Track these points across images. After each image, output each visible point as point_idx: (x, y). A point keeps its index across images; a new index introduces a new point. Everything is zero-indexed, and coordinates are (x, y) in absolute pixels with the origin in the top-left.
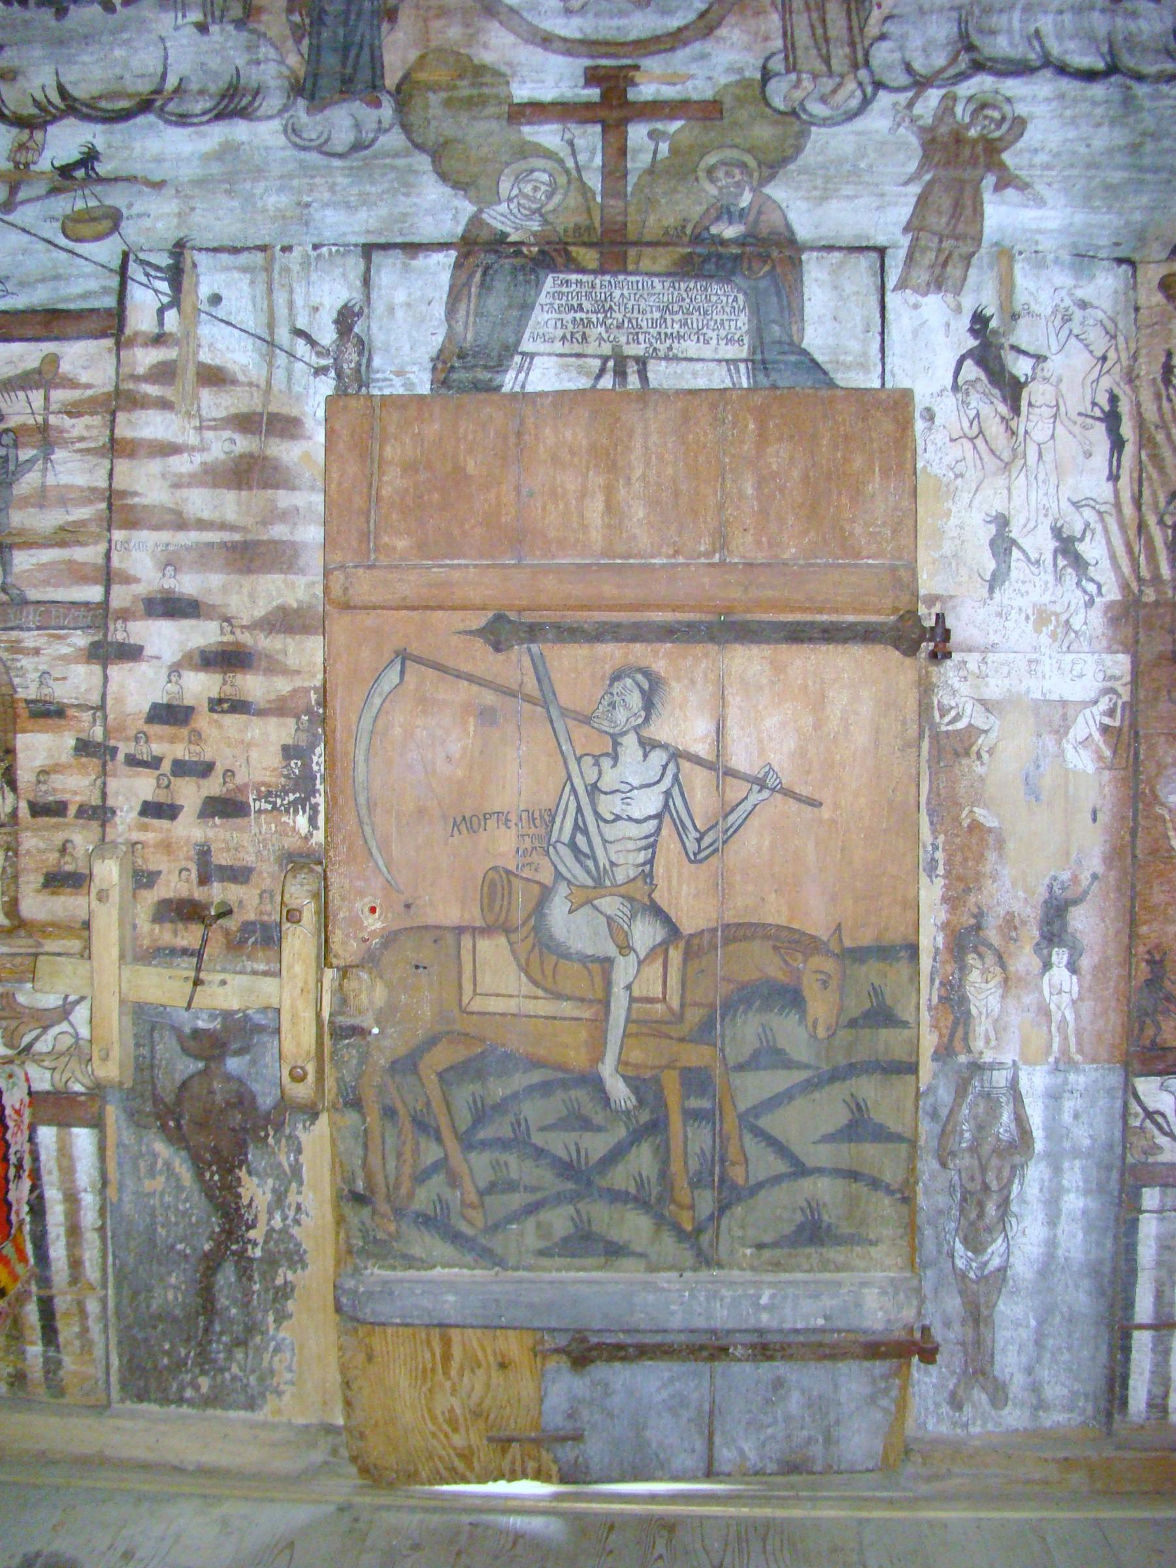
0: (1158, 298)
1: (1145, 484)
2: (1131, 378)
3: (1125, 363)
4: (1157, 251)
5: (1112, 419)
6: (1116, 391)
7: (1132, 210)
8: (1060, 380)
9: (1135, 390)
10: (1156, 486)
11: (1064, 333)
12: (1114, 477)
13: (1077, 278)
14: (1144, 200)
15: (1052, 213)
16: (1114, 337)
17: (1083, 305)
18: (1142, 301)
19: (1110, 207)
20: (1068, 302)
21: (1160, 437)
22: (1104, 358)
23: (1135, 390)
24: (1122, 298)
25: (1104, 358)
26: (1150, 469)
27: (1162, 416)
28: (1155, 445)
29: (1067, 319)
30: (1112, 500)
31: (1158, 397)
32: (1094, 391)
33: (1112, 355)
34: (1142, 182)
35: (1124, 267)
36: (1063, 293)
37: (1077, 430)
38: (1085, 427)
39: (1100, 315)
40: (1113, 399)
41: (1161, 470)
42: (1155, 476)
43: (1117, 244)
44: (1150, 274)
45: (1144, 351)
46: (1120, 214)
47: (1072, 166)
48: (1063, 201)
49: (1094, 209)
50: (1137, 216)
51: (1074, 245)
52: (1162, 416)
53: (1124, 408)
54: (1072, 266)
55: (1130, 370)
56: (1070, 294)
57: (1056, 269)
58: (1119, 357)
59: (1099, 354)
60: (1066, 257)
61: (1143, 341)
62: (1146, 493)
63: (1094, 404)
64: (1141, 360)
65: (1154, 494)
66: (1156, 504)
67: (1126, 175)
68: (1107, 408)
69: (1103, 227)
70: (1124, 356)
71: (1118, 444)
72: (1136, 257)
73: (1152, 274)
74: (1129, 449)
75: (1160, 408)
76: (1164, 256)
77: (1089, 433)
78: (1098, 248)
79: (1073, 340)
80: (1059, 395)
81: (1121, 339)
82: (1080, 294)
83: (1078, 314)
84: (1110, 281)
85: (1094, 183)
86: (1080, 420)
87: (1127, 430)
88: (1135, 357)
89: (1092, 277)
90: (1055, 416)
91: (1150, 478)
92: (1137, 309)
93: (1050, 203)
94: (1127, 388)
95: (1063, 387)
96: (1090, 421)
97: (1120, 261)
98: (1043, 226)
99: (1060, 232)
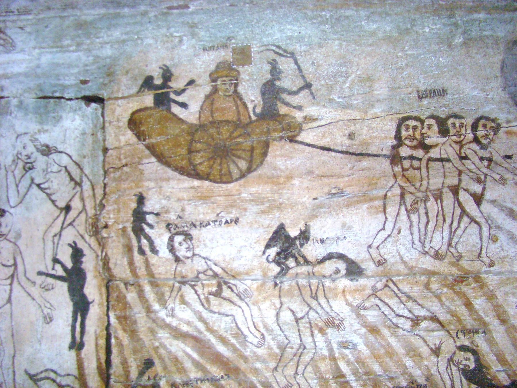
0: (129, 136)
1: (115, 350)
2: (96, 229)
3: (91, 212)
4: (127, 86)
5: (75, 278)
6: (81, 245)
7: (103, 44)
8: (19, 236)
9: (102, 244)
10: (127, 353)
11: (26, 182)
12: (77, 345)
13: (41, 123)
14: (117, 34)
15: (21, 56)
16: (79, 184)
17: (47, 150)
18: (111, 142)
19: (79, 45)
20: (31, 149)
21: (131, 296)
22: (68, 208)
23: (102, 244)
24: (90, 140)
25: (68, 208)
26: (121, 333)
27: (134, 272)
28: (126, 306)
29: (29, 167)
30: (75, 372)
31: (129, 249)
32: (56, 246)
33: (76, 204)
34: (117, 16)
35: (93, 105)
36: (26, 139)
37: (35, 291)
38: (47, 289)
39: (65, 160)
40: (77, 254)
41: (133, 333)
42: (125, 339)
43: (84, 82)
44: (119, 110)
45: (113, 197)
46: (89, 50)
47: (49, 9)
48: (33, 44)
49: (63, 49)
50: (108, 51)
51: (40, 87)
52: (134, 272)
53: (89, 264)
54: (36, 111)
55: (96, 218)
56: (34, 140)
57: (20, 114)
58: (83, 206)
59: (62, 204)
60: (30, 100)
61: (112, 185)
62: (115, 359)
63: (56, 261)
64: (108, 208)
65: (124, 363)
66: (127, 373)
67: (103, 11)
68: (69, 265)
69: (70, 66)
70: (89, 205)
71: (81, 306)
72: (104, 94)
73: (122, 111)
74: (95, 312)
75: (131, 263)
76: (135, 90)
77: (48, 295)
78: (64, 87)
79: (35, 188)
80: (17, 253)
81: (86, 185)
82: (44, 139)
83: (41, 161)
84: (78, 121)
85: (67, 23)
86: (40, 280)
87: (92, 290)
88: (102, 206)
89: (58, 119)
90: (12, 276)
91: (120, 345)
92: (106, 150)
93: (20, 45)
94: (93, 241)
95: (21, 243)
96: (50, 280)
97: (89, 100)
98: (9, 70)
99: (26, 75)
